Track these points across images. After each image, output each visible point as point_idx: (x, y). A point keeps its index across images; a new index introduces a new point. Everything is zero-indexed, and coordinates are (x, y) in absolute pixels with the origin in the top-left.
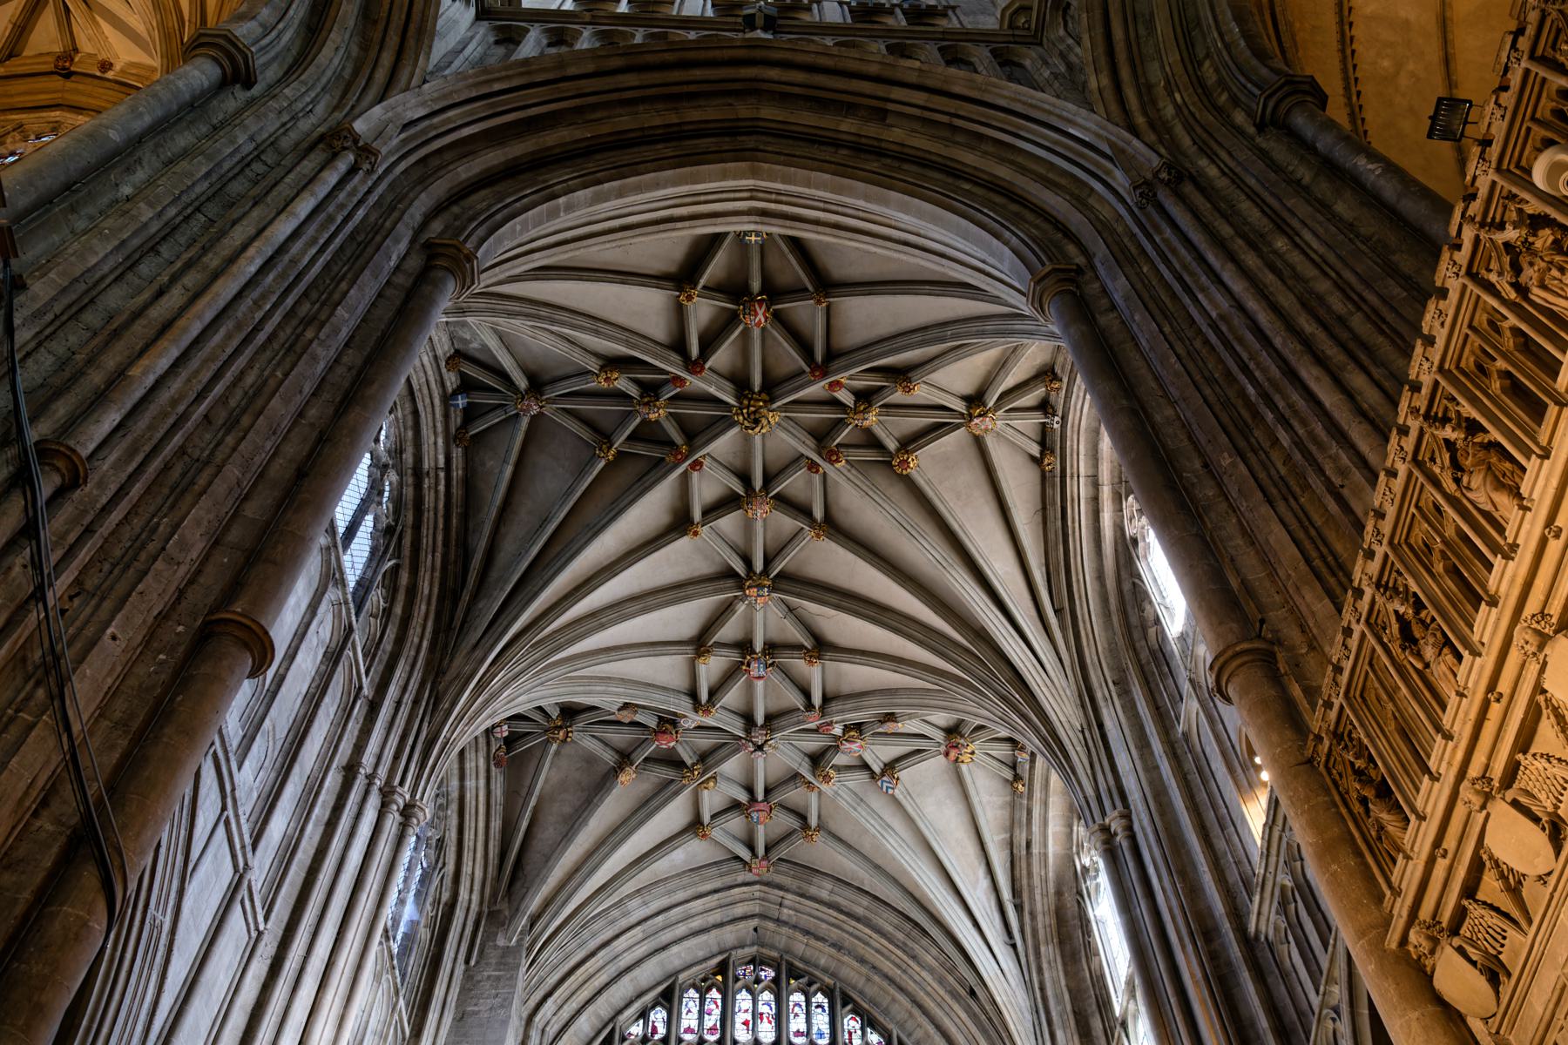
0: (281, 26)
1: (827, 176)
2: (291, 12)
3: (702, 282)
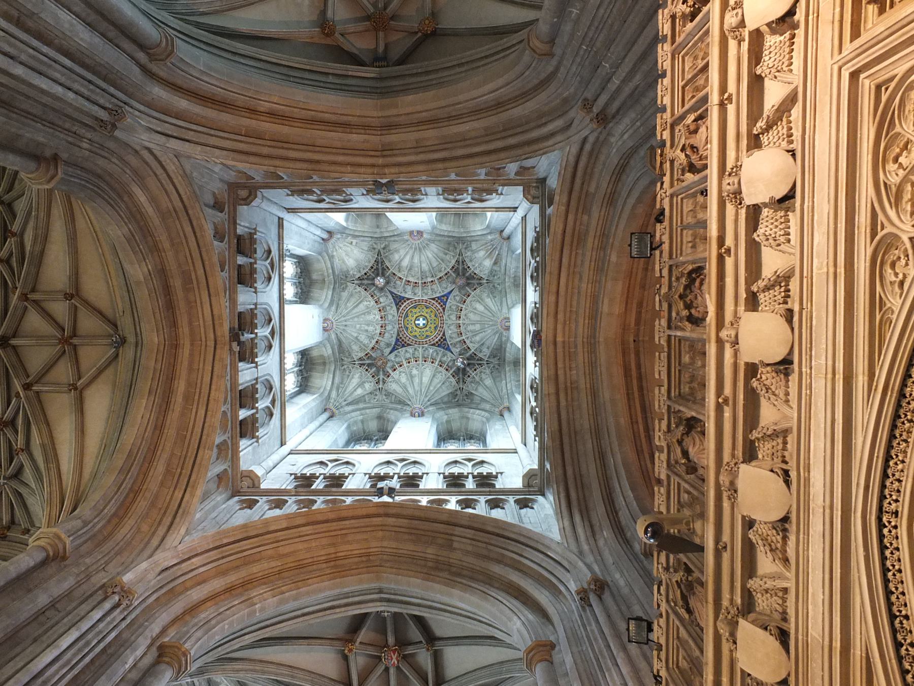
0: (96, 520)
1: (419, 581)
2: (106, 511)
3: (359, 640)
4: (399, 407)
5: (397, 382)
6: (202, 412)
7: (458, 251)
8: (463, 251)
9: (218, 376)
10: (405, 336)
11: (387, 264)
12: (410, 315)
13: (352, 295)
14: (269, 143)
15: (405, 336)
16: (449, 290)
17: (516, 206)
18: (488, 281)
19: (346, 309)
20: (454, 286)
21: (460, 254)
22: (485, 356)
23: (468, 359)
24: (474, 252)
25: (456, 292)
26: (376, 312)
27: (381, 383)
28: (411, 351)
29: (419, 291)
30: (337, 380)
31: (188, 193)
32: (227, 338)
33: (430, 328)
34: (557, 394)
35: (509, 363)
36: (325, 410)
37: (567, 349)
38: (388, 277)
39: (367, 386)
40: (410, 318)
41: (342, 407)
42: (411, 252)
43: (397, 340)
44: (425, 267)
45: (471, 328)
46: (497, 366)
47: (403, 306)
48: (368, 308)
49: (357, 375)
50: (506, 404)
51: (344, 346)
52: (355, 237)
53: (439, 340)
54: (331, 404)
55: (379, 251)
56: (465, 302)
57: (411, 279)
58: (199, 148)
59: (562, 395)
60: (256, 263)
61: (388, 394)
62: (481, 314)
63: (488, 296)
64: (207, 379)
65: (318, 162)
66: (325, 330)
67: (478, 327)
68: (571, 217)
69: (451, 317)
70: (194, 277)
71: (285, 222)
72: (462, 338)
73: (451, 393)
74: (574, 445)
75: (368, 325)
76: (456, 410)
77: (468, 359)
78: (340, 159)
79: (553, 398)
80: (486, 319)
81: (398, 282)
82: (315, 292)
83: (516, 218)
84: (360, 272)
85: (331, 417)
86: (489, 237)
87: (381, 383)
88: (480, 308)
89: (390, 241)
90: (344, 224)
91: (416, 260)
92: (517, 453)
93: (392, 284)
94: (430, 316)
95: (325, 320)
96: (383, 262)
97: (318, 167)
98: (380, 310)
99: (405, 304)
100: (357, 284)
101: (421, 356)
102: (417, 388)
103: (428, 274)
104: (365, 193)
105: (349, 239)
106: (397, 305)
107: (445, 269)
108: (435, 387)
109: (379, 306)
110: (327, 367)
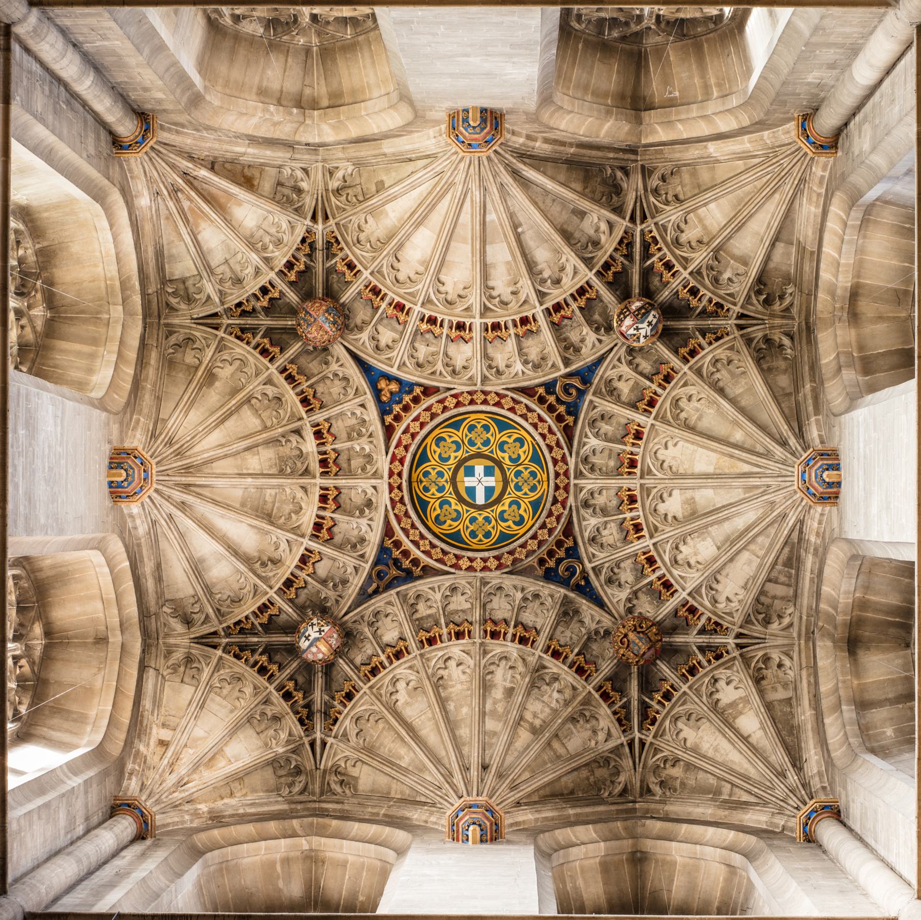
10: (532, 545)
11: (248, 608)
12: (449, 526)
13: (370, 750)
20: (338, 350)
21: (211, 321)
26: (436, 654)
27: (718, 640)
33: (502, 446)
38: (301, 609)
46: (654, 182)
47: (416, 553)
57: (308, 519)
84: (276, 718)
86: (144, 201)
87: (718, 640)
89: (160, 594)
93: (327, 593)
98: (431, 641)
99: (407, 544)
101: (614, 483)
108: (736, 423)
109: (412, 644)
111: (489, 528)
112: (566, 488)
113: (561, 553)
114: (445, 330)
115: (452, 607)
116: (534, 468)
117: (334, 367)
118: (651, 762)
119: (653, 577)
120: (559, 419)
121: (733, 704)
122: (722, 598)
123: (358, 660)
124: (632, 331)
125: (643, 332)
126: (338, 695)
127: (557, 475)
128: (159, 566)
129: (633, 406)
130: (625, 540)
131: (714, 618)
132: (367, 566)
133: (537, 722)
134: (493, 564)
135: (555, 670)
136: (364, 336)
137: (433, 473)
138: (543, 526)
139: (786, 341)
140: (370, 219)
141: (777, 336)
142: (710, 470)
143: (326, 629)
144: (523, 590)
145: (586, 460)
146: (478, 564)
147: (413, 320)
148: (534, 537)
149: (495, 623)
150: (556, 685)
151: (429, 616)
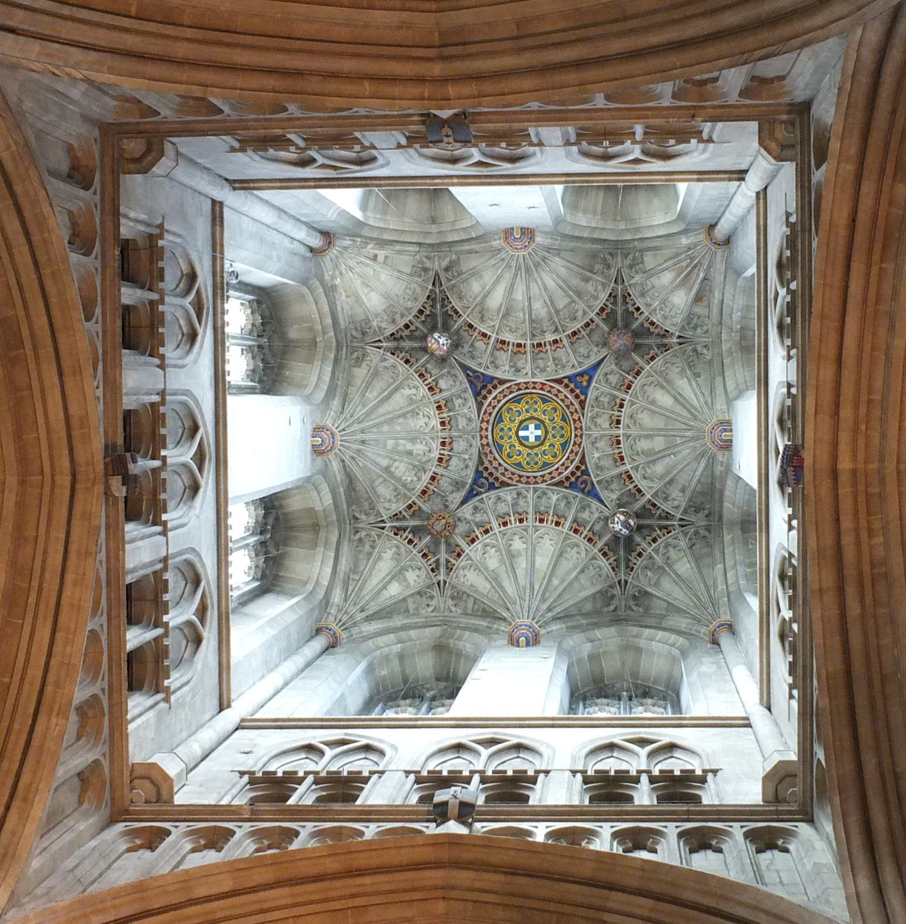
4: (484, 624)
5: (480, 568)
6: (44, 633)
7: (613, 272)
8: (625, 273)
9: (79, 553)
10: (495, 464)
11: (455, 303)
12: (506, 416)
13: (376, 374)
14: (189, 33)
15: (495, 464)
16: (594, 360)
17: (744, 167)
18: (683, 340)
19: (364, 406)
20: (604, 352)
21: (619, 280)
22: (677, 507)
23: (638, 516)
24: (649, 274)
25: (609, 366)
26: (432, 411)
27: (442, 570)
28: (509, 498)
29: (526, 363)
30: (344, 564)
31: (14, 148)
32: (100, 467)
33: (552, 445)
34: (841, 590)
35: (732, 524)
36: (318, 631)
37: (861, 487)
38: (457, 332)
39: (411, 576)
40: (506, 424)
41: (355, 624)
42: (508, 276)
43: (478, 474)
44: (540, 309)
45: (644, 445)
47: (490, 398)
48: (411, 401)
49: (388, 554)
50: (725, 617)
51: (359, 487)
52: (382, 243)
53: (573, 473)
54: (331, 618)
55: (437, 275)
56: (629, 387)
58: (36, 46)
59: (851, 592)
60: (162, 301)
61: (458, 596)
62: (666, 415)
63: (682, 372)
64: (56, 560)
65: (298, 73)
66: (317, 451)
67: (659, 443)
68: (868, 188)
69: (599, 421)
70: (25, 332)
71: (226, 211)
72: (622, 469)
73: (600, 592)
74: (880, 705)
75: (413, 440)
76: (612, 630)
77: (638, 516)
78: (347, 65)
79: (830, 599)
80: (679, 425)
81: (480, 345)
82: (296, 369)
83: (744, 195)
84: (393, 321)
85: (332, 646)
86: (684, 241)
87: (442, 570)
88: (664, 399)
89: (461, 252)
90: (359, 215)
91: (519, 294)
92: (749, 726)
93: (466, 349)
94: (552, 420)
95: (317, 430)
96: (445, 300)
97: (299, 84)
98: (439, 408)
100: (385, 350)
101: (531, 510)
102: (523, 581)
103: (546, 324)
104: (403, 141)
105: (370, 249)
106: (477, 394)
107: (585, 313)
108: (563, 581)
109: (437, 397)
110: (322, 534)
111: (506, 438)
112: (528, 483)
113: (491, 480)
114: (616, 413)
115: (459, 418)
116: (540, 464)
117: (595, 349)
118: (373, 533)
119: (477, 533)
120: (567, 478)
121: (405, 579)
122: (466, 572)
123: (429, 366)
124: (616, 519)
125: (616, 526)
126: (408, 355)
127: (535, 477)
128: (476, 252)
129: (575, 521)
130: (499, 516)
131: (454, 568)
132: (482, 370)
133: (393, 469)
134: (484, 441)
135: (424, 478)
136: (613, 367)
137: (536, 406)
138: (506, 470)
139: (612, 608)
140: (680, 369)
141: (615, 603)
142: (537, 566)
143: (445, 348)
144: (470, 459)
145: (544, 493)
146: (484, 433)
147: (621, 395)
148: (500, 465)
149: (450, 443)
150: (415, 479)
151: (454, 406)
